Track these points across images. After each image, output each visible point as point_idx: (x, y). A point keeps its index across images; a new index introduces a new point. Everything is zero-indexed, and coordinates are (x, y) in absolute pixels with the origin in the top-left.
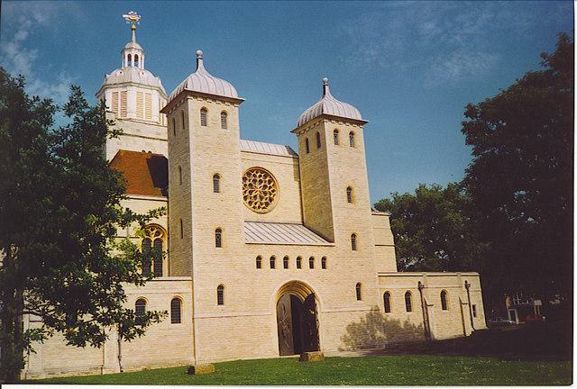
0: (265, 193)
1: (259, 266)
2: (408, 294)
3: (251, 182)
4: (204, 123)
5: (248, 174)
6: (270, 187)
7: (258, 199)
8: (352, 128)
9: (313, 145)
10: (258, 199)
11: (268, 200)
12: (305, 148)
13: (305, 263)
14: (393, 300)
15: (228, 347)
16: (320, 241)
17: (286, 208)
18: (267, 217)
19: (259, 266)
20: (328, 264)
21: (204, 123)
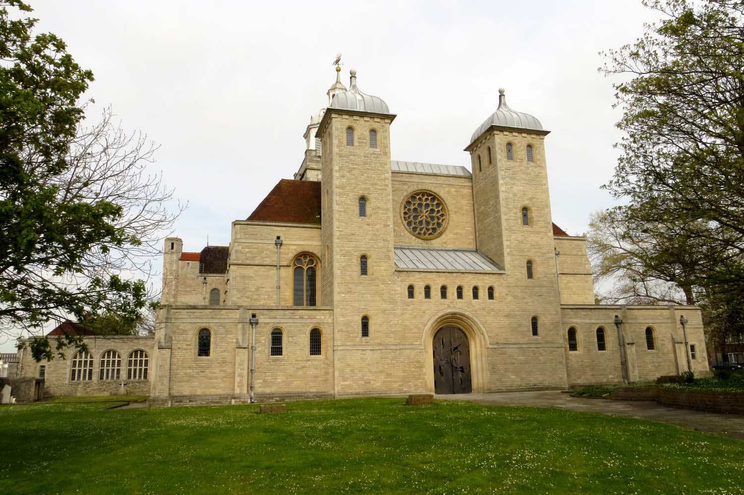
0: (432, 218)
1: (411, 294)
2: (600, 333)
3: (416, 206)
4: (350, 142)
5: (413, 197)
6: (438, 212)
8: (529, 139)
9: (485, 162)
10: (424, 225)
11: (435, 226)
12: (477, 166)
13: (468, 293)
14: (580, 337)
16: (488, 267)
17: (457, 234)
18: (436, 243)
19: (411, 294)
20: (496, 294)
21: (350, 142)
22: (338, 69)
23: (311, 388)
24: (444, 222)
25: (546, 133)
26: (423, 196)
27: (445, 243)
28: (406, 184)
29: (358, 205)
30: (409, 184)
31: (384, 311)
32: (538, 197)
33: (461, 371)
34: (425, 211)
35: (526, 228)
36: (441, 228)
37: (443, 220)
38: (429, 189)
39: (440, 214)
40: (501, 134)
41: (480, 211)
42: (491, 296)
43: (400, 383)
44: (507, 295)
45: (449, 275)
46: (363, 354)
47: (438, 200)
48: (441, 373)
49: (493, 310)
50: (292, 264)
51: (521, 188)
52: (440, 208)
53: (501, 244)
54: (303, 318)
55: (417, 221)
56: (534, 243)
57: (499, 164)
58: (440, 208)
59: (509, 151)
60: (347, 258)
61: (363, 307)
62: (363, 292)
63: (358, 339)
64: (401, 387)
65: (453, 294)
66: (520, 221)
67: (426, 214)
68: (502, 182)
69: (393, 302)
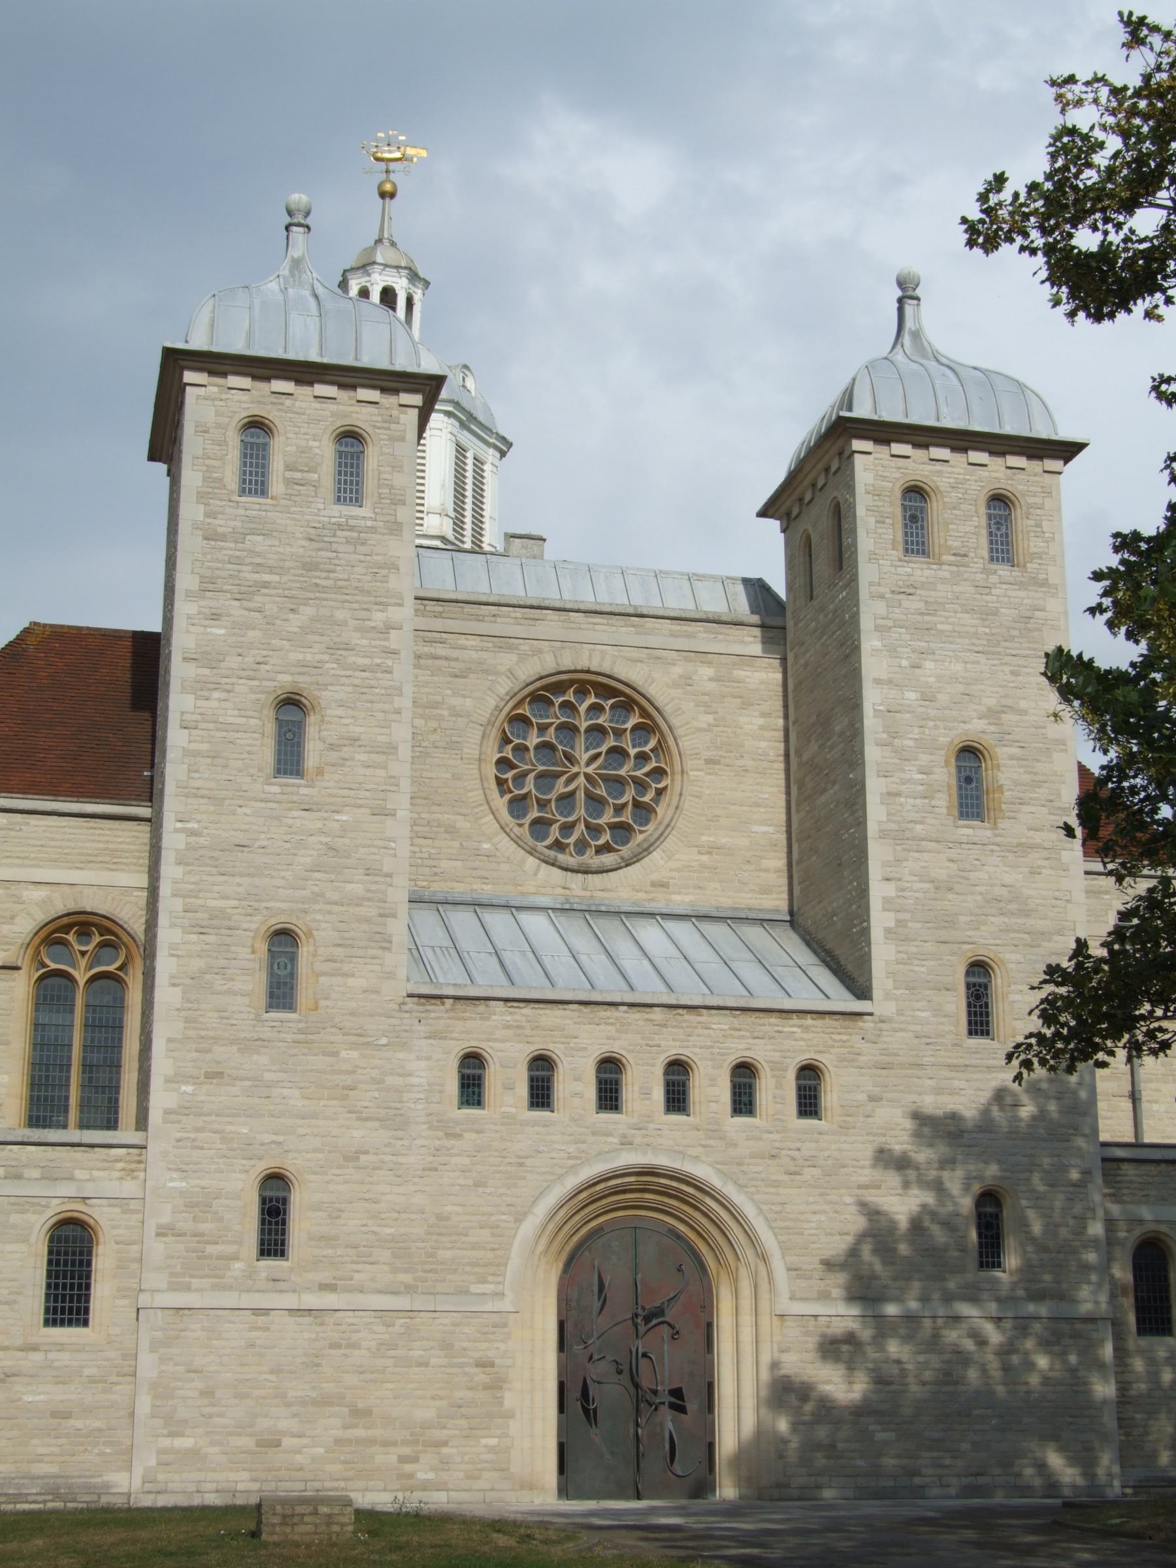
3: (551, 736)
6: (642, 757)
7: (581, 811)
9: (822, 567)
10: (581, 811)
15: (287, 1442)
17: (710, 850)
20: (830, 1098)
22: (388, 187)
23: (39, 1459)
24: (665, 799)
25: (1068, 450)
26: (582, 692)
27: (664, 885)
28: (511, 648)
29: (270, 728)
30: (525, 647)
31: (352, 1157)
32: (1023, 704)
33: (672, 1406)
34: (585, 757)
35: (968, 830)
36: (650, 827)
37: (660, 792)
38: (606, 669)
39: (647, 769)
40: (881, 453)
41: (805, 758)
42: (809, 1104)
43: (406, 1451)
44: (873, 1099)
45: (635, 1016)
46: (254, 1328)
47: (644, 713)
48: (586, 1411)
49: (812, 1162)
50: (25, 963)
51: (959, 667)
52: (652, 743)
53: (863, 893)
54: (19, 1177)
55: (553, 796)
56: (998, 891)
57: (867, 573)
58: (652, 743)
59: (914, 519)
60: (212, 939)
61: (268, 1138)
62: (268, 1076)
63: (238, 1265)
64: (408, 1468)
65: (646, 1093)
66: (944, 802)
67: (590, 770)
68: (877, 644)
69: (396, 1121)
